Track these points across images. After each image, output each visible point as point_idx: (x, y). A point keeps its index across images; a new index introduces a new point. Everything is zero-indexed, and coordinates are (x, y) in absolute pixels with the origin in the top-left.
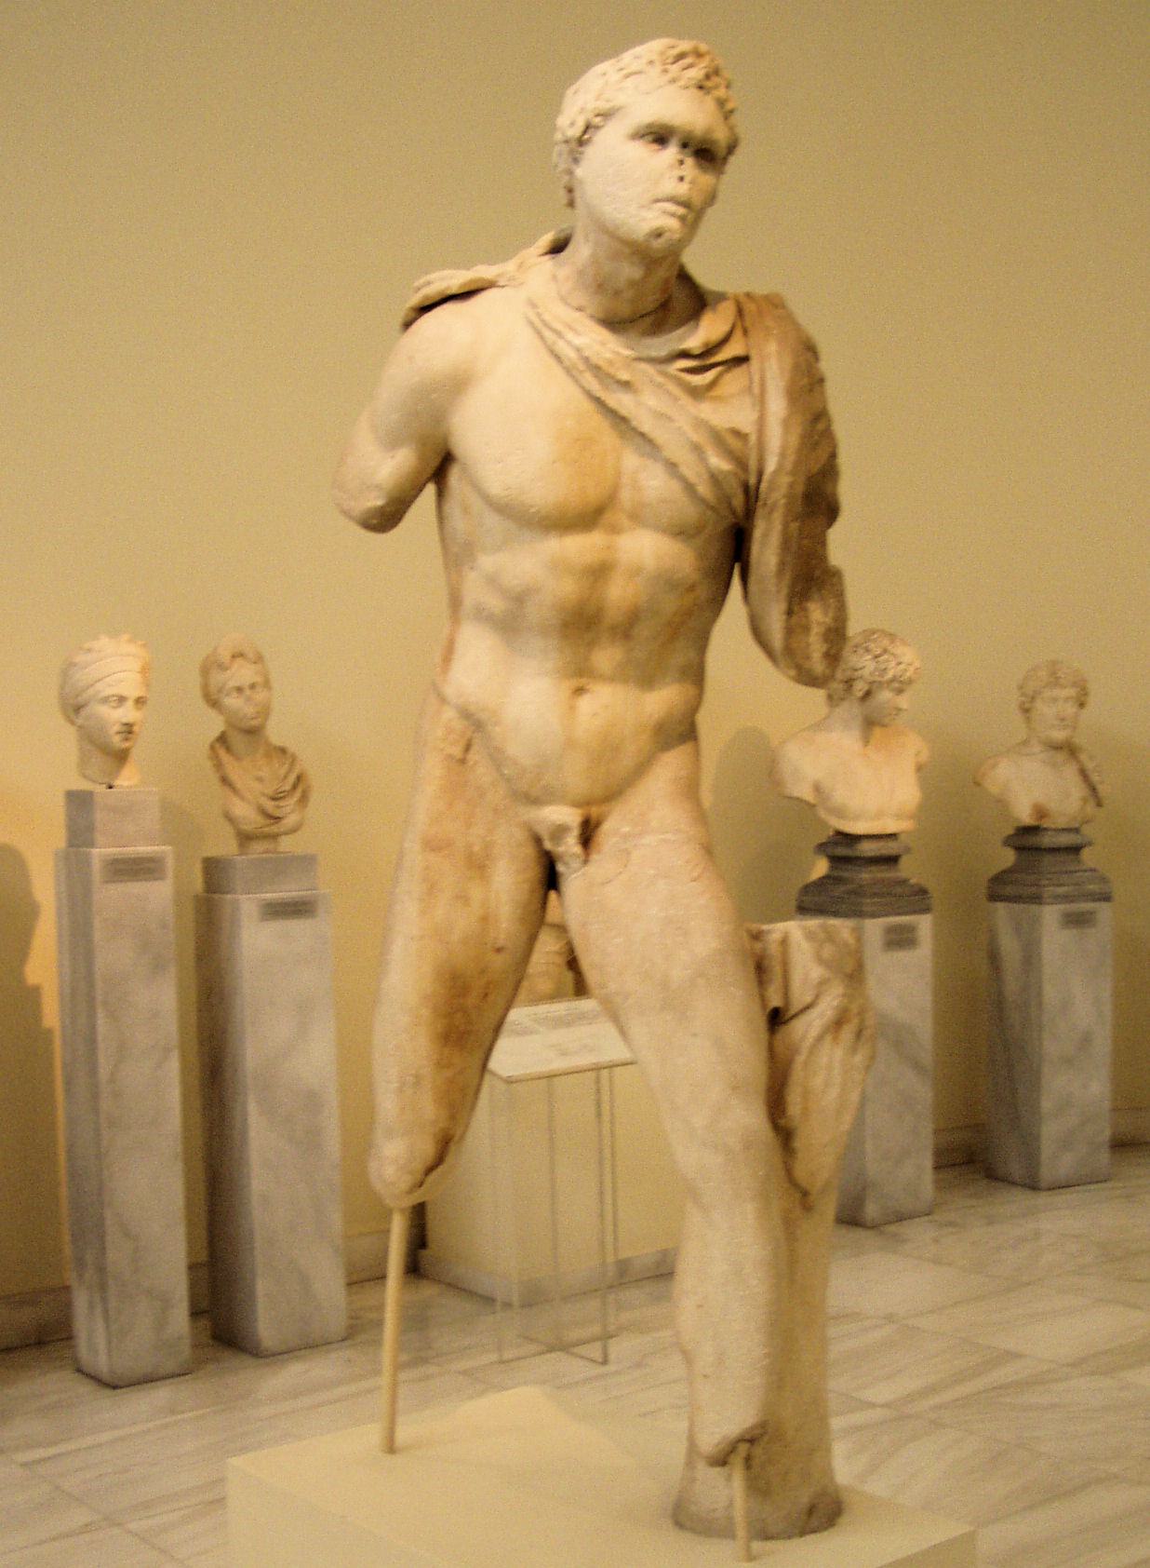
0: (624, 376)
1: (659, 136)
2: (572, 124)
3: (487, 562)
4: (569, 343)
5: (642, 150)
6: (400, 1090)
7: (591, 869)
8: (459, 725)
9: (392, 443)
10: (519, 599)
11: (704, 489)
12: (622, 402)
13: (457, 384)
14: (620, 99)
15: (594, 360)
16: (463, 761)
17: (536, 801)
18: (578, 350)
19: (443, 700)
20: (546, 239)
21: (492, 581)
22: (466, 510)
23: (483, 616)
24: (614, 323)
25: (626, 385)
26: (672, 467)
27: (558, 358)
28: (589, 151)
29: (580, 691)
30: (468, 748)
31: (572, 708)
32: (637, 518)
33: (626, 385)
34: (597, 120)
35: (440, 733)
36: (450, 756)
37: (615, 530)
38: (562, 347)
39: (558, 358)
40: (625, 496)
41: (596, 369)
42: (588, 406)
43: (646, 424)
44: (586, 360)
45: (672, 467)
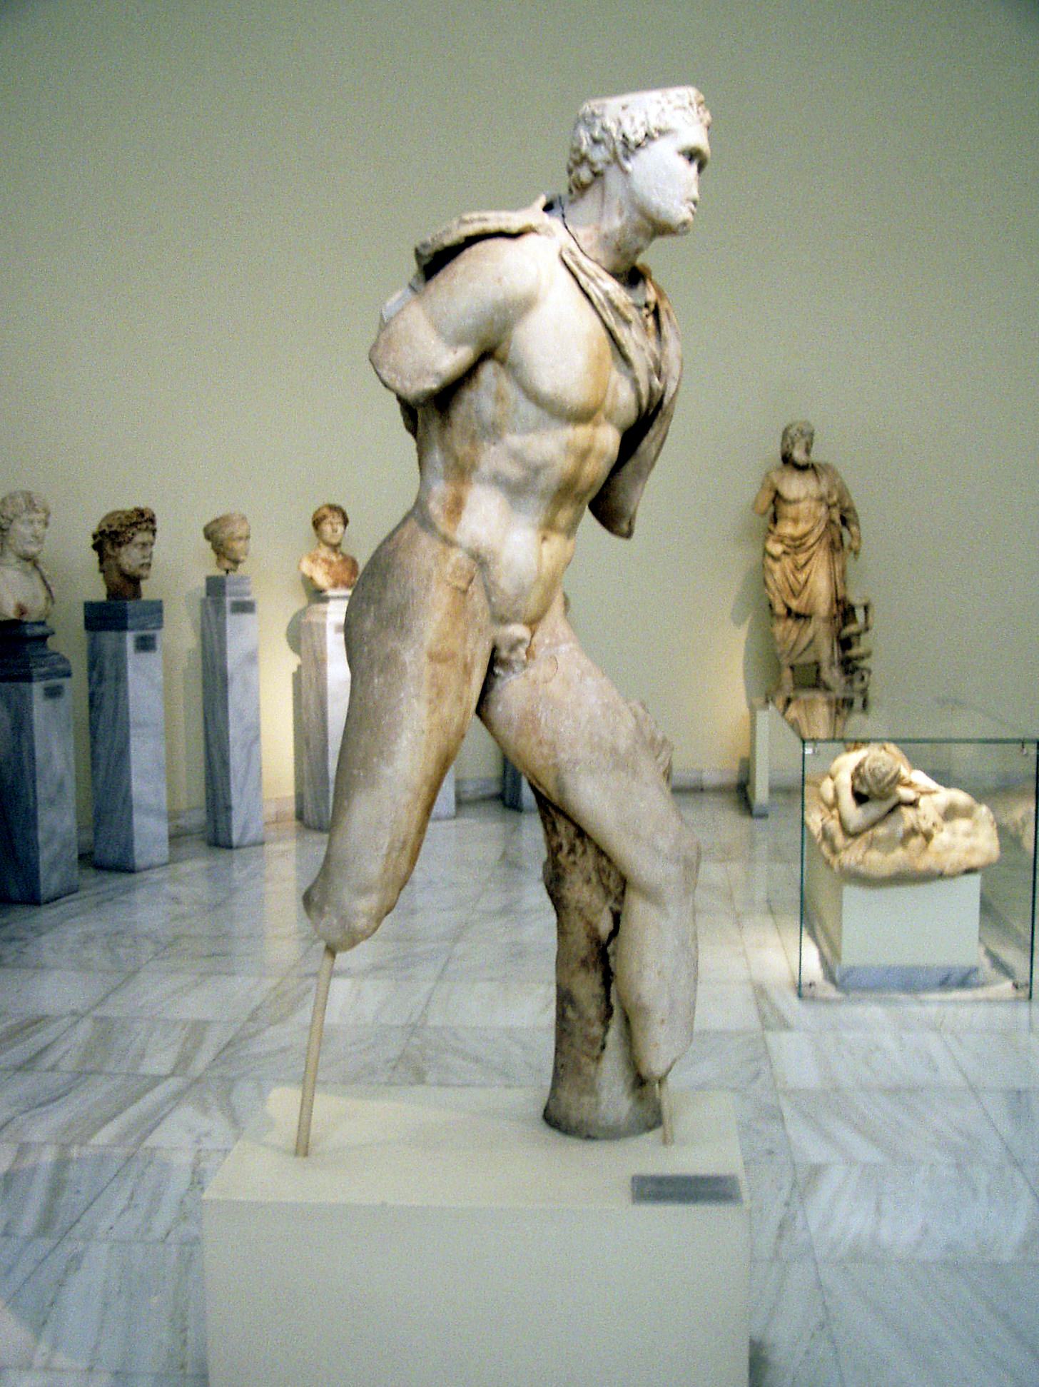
0: (630, 316)
1: (693, 155)
2: (636, 132)
3: (514, 440)
4: (599, 287)
5: (682, 162)
6: (388, 854)
7: (532, 672)
8: (466, 563)
9: (458, 340)
10: (537, 470)
11: (645, 402)
12: (622, 333)
13: (524, 306)
14: (673, 124)
15: (616, 302)
16: (465, 592)
17: (503, 620)
18: (606, 294)
19: (448, 542)
20: (542, 201)
21: (516, 456)
22: (499, 398)
23: (498, 480)
24: (615, 275)
25: (627, 322)
26: (635, 382)
27: (587, 296)
28: (642, 154)
29: (544, 539)
30: (471, 581)
31: (540, 551)
32: (609, 418)
33: (627, 322)
34: (656, 135)
35: (449, 569)
36: (457, 588)
37: (597, 425)
38: (592, 289)
39: (587, 296)
40: (608, 403)
41: (615, 309)
42: (604, 334)
43: (631, 351)
44: (611, 302)
45: (635, 382)
